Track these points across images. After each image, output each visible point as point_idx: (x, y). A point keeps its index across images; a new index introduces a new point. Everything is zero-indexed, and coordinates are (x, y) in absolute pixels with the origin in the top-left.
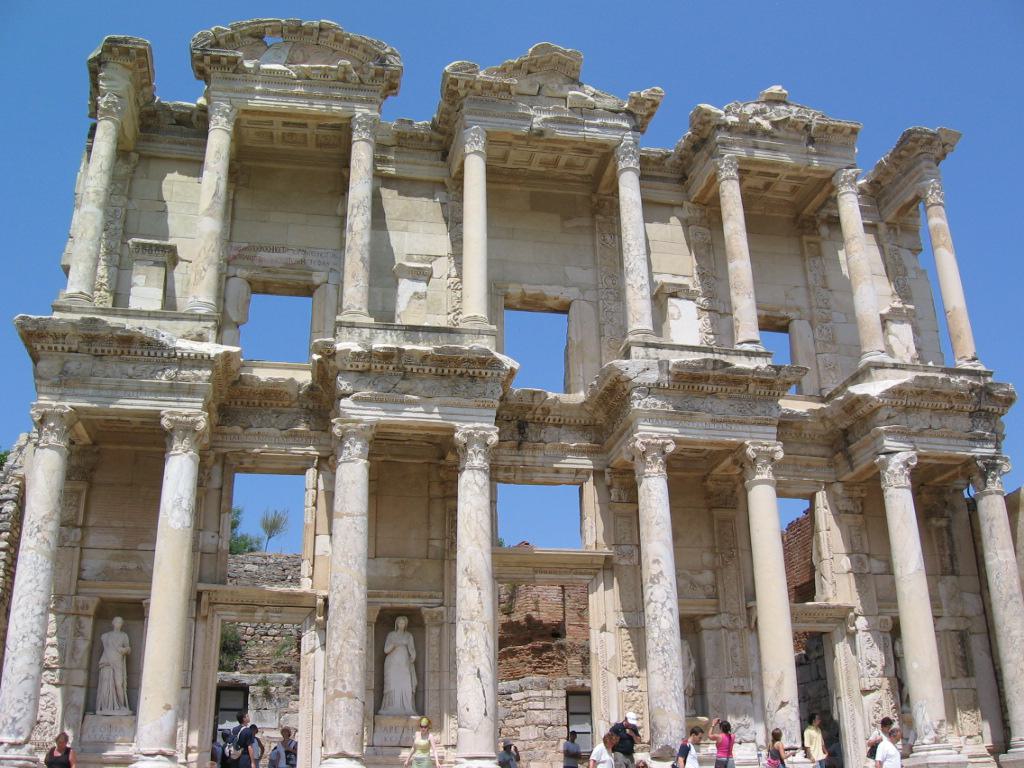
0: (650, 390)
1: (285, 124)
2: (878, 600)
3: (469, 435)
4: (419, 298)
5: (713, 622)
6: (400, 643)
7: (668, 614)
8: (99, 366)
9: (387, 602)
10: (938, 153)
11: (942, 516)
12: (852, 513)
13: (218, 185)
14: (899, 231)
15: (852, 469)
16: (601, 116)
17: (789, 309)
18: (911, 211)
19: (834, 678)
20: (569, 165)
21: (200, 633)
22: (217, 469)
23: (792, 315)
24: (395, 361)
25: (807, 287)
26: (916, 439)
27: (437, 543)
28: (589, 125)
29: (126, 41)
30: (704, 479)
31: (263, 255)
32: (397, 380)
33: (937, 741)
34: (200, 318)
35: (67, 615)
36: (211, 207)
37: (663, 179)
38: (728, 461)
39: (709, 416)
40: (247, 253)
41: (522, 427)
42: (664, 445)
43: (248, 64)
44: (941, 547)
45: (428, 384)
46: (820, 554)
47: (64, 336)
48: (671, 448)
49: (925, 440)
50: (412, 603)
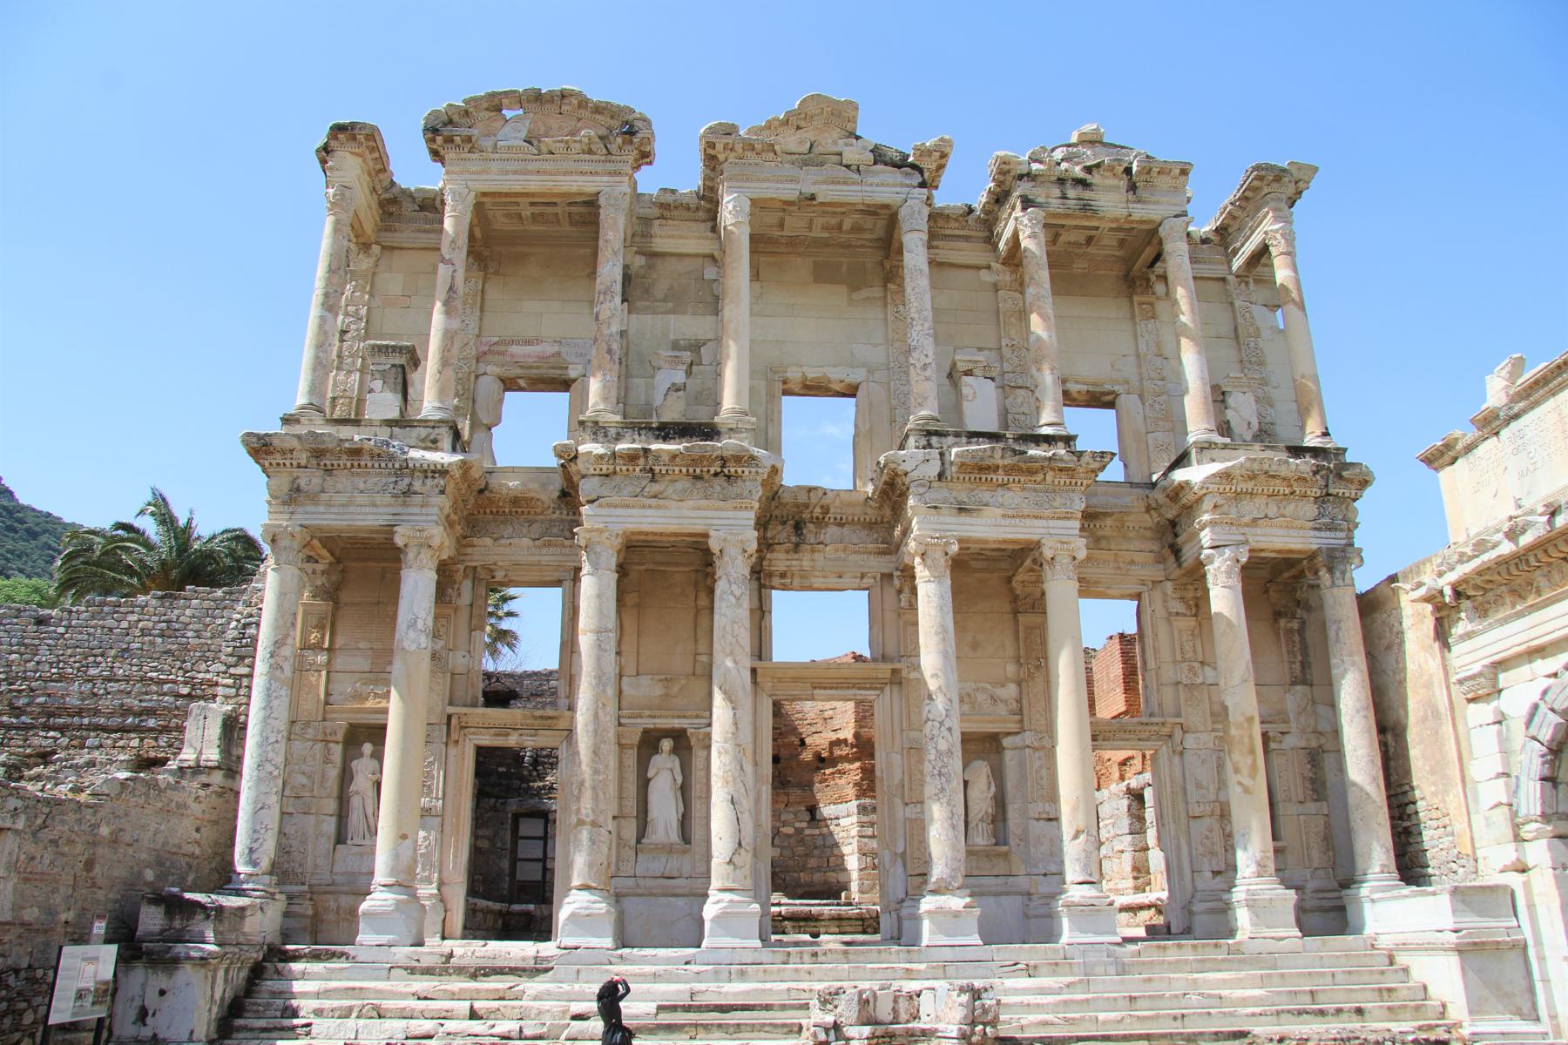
1: (532, 204)
2: (1212, 714)
3: (725, 540)
4: (677, 390)
5: (1017, 740)
6: (664, 768)
7: (946, 733)
8: (330, 481)
9: (650, 723)
10: (1291, 190)
13: (453, 278)
14: (1252, 285)
15: (1180, 565)
17: (1116, 382)
18: (1263, 260)
20: (857, 229)
21: (451, 758)
22: (467, 584)
24: (642, 461)
25: (1138, 356)
26: (1247, 530)
27: (704, 658)
29: (353, 125)
30: (1009, 580)
31: (515, 349)
32: (645, 482)
35: (315, 741)
37: (967, 238)
38: (1028, 562)
39: (999, 511)
40: (495, 348)
41: (798, 527)
42: (948, 544)
43: (487, 143)
44: (1291, 653)
45: (679, 485)
47: (292, 451)
48: (955, 548)
49: (1259, 531)
50: (677, 723)
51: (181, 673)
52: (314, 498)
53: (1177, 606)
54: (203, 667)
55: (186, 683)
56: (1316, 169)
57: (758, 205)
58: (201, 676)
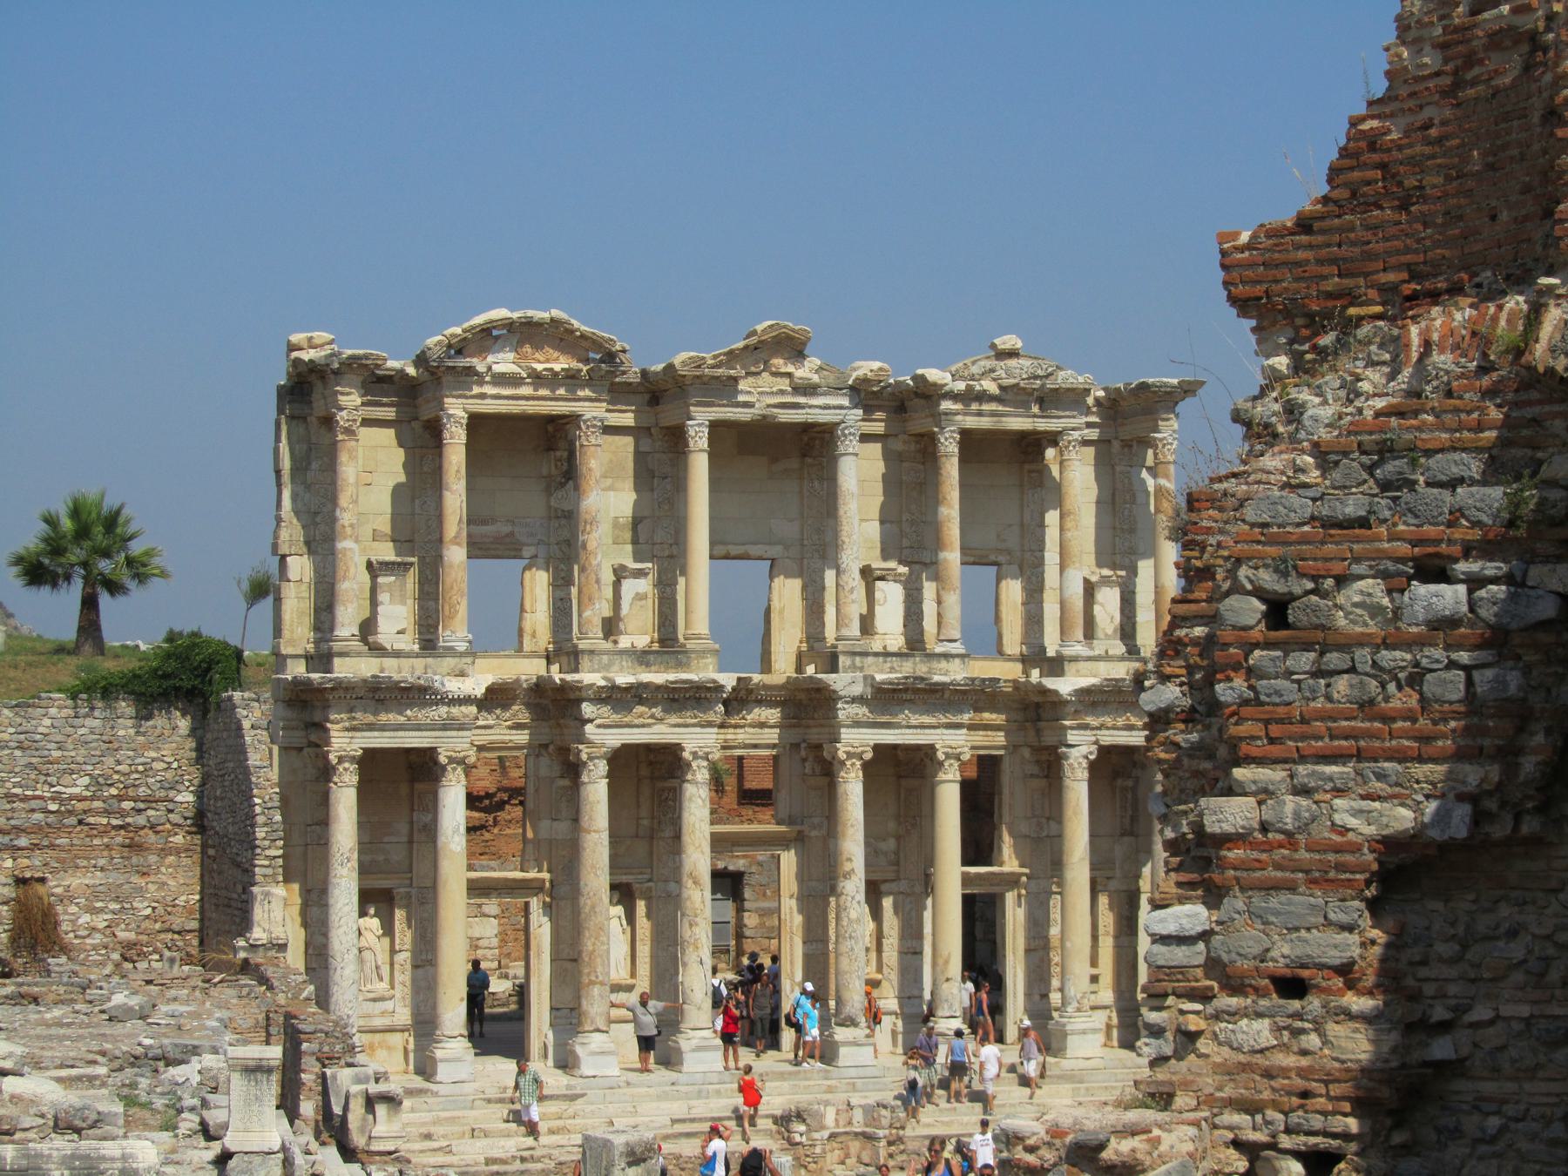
0: (854, 700)
3: (695, 754)
11: (1129, 777)
12: (1038, 776)
16: (824, 394)
17: (1000, 551)
19: (1004, 925)
23: (1001, 559)
25: (1022, 525)
27: (645, 822)
28: (811, 407)
29: (366, 357)
33: (1079, 1010)
34: (462, 655)
36: (458, 533)
43: (481, 368)
46: (1001, 816)
48: (869, 756)
50: (624, 879)
51: (46, 788)
52: (371, 727)
53: (1035, 770)
54: (67, 779)
55: (53, 799)
56: (1203, 383)
57: (715, 426)
58: (69, 790)
